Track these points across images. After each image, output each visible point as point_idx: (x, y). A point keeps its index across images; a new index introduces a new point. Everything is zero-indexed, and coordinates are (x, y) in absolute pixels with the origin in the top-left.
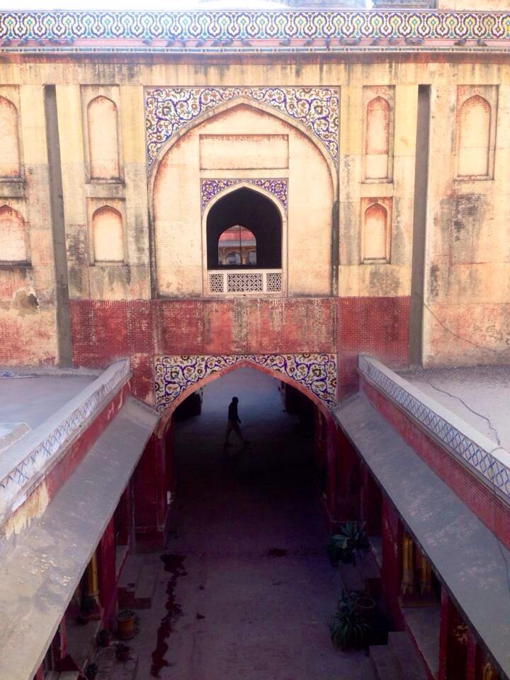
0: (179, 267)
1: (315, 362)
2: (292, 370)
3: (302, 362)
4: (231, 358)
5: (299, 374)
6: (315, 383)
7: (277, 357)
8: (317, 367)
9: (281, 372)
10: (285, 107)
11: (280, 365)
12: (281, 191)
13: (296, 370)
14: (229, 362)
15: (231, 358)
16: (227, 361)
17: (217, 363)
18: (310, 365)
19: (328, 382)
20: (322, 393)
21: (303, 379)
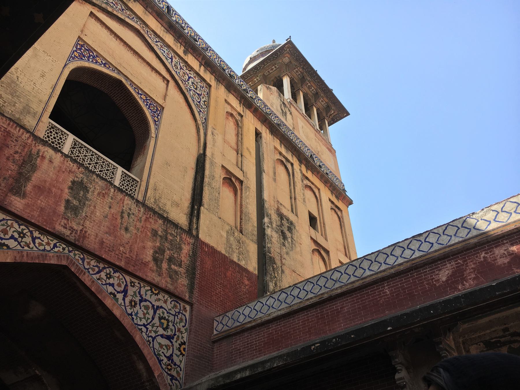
0: (13, 82)
1: (164, 305)
2: (133, 304)
3: (148, 297)
4: (46, 240)
5: (141, 315)
6: (159, 339)
7: (117, 275)
8: (166, 315)
9: (117, 300)
10: (171, 62)
11: (119, 289)
12: (155, 112)
13: (138, 305)
14: (40, 244)
15: (46, 240)
16: (37, 241)
17: (16, 235)
18: (158, 307)
19: (176, 345)
20: (165, 360)
21: (144, 325)
